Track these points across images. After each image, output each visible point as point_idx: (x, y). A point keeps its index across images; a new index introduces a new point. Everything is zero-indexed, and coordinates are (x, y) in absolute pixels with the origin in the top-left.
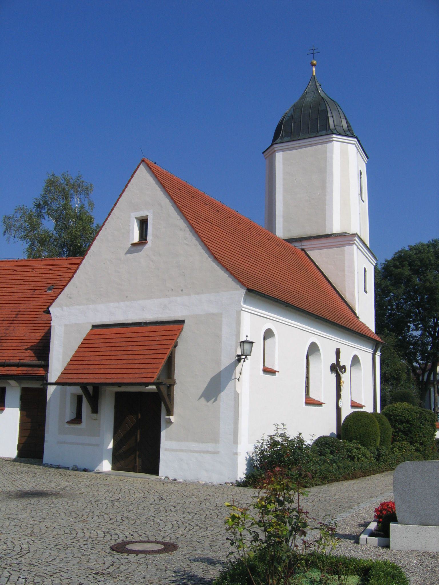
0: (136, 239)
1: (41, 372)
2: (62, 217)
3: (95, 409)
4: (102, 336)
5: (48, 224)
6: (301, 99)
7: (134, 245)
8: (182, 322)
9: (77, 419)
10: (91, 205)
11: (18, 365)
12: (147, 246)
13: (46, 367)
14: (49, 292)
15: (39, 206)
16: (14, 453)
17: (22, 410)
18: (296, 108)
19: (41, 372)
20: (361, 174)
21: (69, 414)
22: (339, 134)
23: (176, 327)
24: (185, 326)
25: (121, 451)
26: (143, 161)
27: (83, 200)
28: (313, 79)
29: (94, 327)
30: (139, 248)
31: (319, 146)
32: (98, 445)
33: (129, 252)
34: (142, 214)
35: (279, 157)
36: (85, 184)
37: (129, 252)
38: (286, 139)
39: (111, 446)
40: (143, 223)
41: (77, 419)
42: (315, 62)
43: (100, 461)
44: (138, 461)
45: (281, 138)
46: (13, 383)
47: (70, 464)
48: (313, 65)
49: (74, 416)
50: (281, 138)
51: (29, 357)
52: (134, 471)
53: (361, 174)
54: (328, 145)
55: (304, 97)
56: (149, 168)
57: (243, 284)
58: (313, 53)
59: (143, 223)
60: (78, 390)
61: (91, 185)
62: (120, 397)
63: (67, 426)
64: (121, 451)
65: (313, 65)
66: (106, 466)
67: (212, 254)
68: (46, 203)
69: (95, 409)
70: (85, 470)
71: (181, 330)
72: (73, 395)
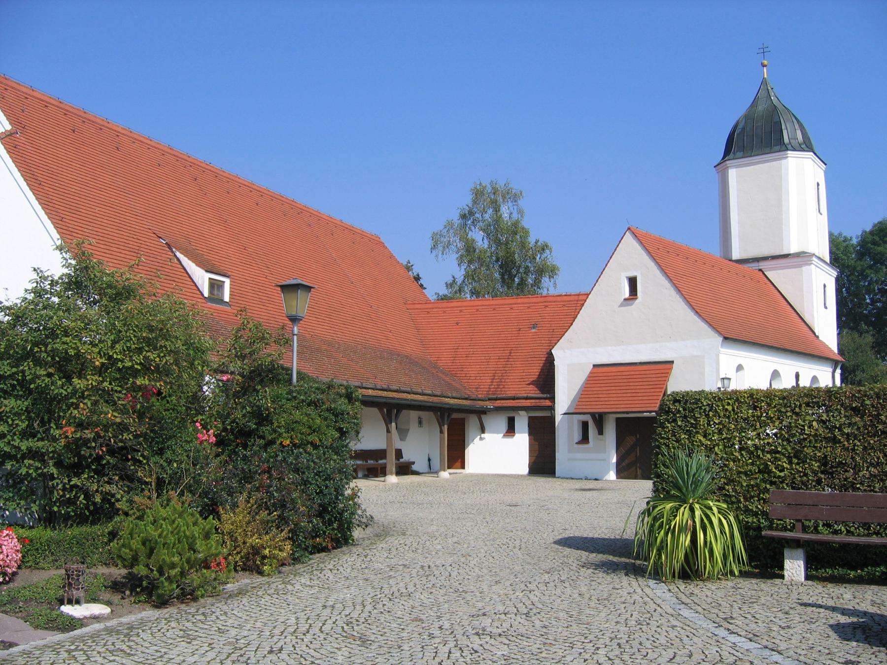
0: (627, 295)
1: (548, 403)
2: (494, 230)
3: (601, 432)
4: (602, 375)
5: (478, 237)
6: (752, 106)
7: (625, 299)
8: (673, 362)
9: (585, 439)
10: (521, 212)
11: (527, 398)
12: (637, 301)
13: (552, 399)
14: (533, 330)
15: (463, 217)
16: (525, 470)
17: (530, 434)
18: (749, 117)
19: (548, 403)
20: (818, 185)
21: (577, 436)
22: (795, 150)
23: (667, 366)
24: (674, 365)
25: (624, 464)
26: (629, 229)
27: (511, 209)
28: (764, 82)
29: (594, 366)
30: (631, 302)
31: (774, 163)
32: (605, 460)
33: (621, 305)
34: (632, 274)
35: (733, 174)
36: (514, 191)
37: (621, 305)
38: (739, 154)
39: (614, 460)
40: (633, 282)
41: (585, 439)
42: (766, 62)
43: (608, 472)
44: (639, 472)
45: (734, 153)
46: (523, 413)
47: (582, 476)
48: (764, 66)
49: (581, 438)
50: (734, 153)
51: (533, 391)
52: (636, 478)
53: (818, 185)
54: (783, 161)
55: (754, 103)
56: (635, 235)
57: (720, 333)
58: (764, 51)
59: (633, 282)
60: (588, 418)
61: (521, 192)
62: (618, 420)
63: (576, 446)
64: (624, 464)
65: (764, 66)
66: (612, 476)
67: (694, 309)
68: (471, 213)
69: (601, 432)
70: (596, 479)
71: (671, 369)
72: (579, 421)
